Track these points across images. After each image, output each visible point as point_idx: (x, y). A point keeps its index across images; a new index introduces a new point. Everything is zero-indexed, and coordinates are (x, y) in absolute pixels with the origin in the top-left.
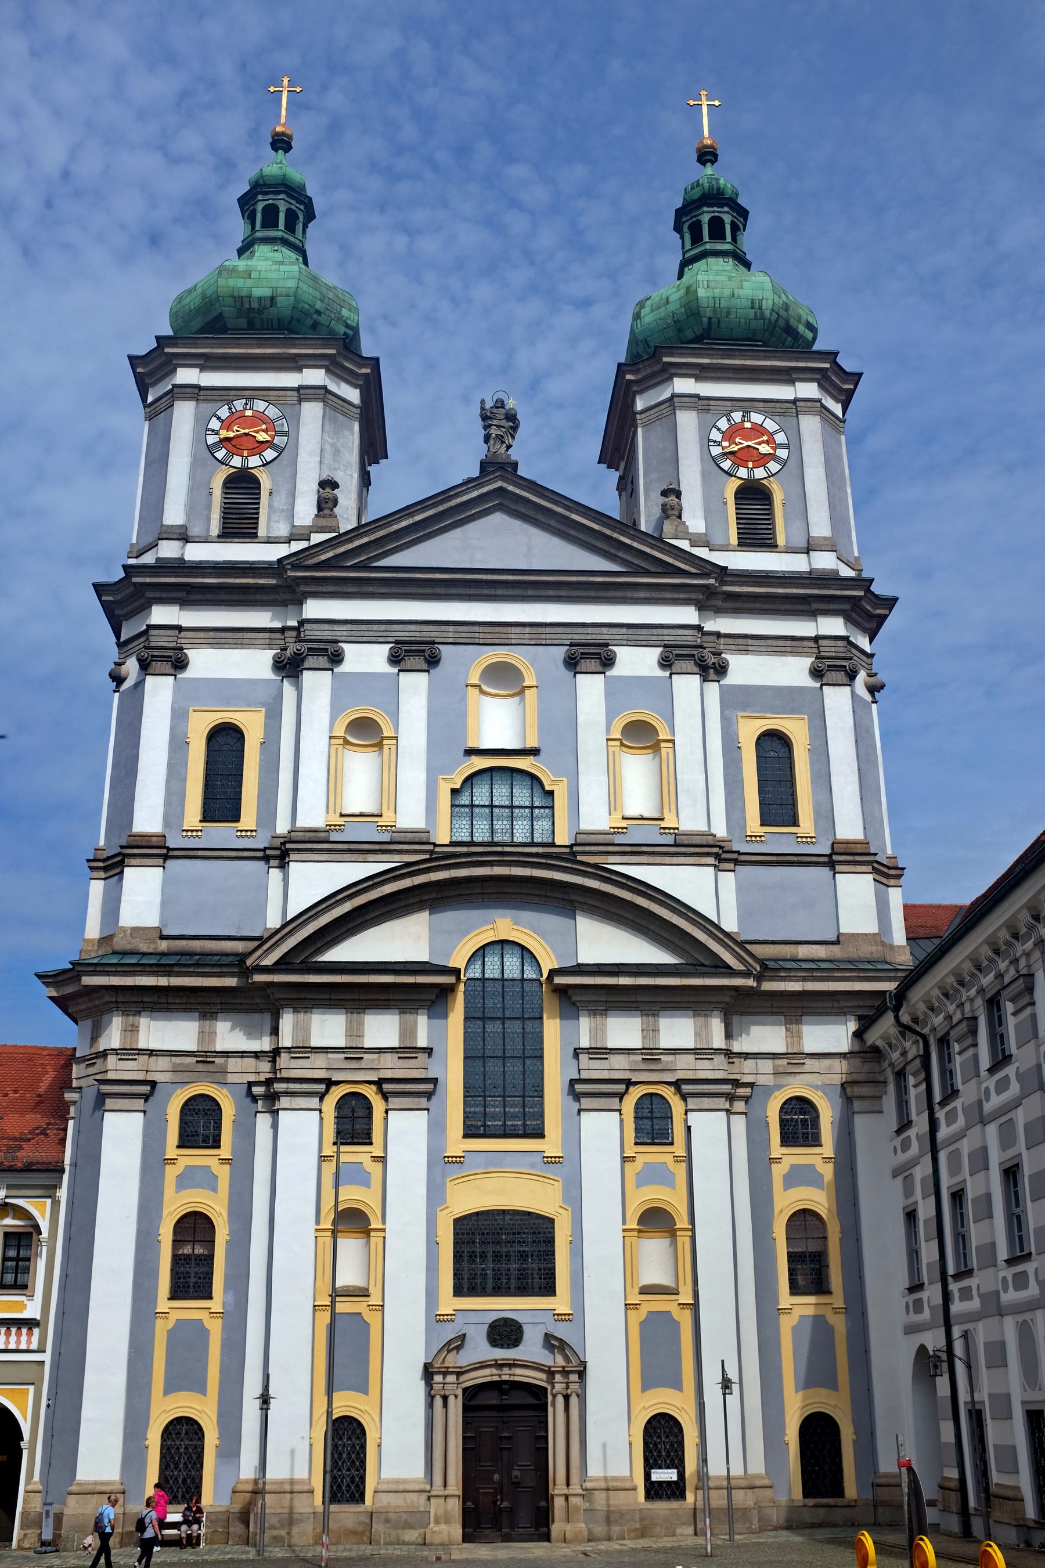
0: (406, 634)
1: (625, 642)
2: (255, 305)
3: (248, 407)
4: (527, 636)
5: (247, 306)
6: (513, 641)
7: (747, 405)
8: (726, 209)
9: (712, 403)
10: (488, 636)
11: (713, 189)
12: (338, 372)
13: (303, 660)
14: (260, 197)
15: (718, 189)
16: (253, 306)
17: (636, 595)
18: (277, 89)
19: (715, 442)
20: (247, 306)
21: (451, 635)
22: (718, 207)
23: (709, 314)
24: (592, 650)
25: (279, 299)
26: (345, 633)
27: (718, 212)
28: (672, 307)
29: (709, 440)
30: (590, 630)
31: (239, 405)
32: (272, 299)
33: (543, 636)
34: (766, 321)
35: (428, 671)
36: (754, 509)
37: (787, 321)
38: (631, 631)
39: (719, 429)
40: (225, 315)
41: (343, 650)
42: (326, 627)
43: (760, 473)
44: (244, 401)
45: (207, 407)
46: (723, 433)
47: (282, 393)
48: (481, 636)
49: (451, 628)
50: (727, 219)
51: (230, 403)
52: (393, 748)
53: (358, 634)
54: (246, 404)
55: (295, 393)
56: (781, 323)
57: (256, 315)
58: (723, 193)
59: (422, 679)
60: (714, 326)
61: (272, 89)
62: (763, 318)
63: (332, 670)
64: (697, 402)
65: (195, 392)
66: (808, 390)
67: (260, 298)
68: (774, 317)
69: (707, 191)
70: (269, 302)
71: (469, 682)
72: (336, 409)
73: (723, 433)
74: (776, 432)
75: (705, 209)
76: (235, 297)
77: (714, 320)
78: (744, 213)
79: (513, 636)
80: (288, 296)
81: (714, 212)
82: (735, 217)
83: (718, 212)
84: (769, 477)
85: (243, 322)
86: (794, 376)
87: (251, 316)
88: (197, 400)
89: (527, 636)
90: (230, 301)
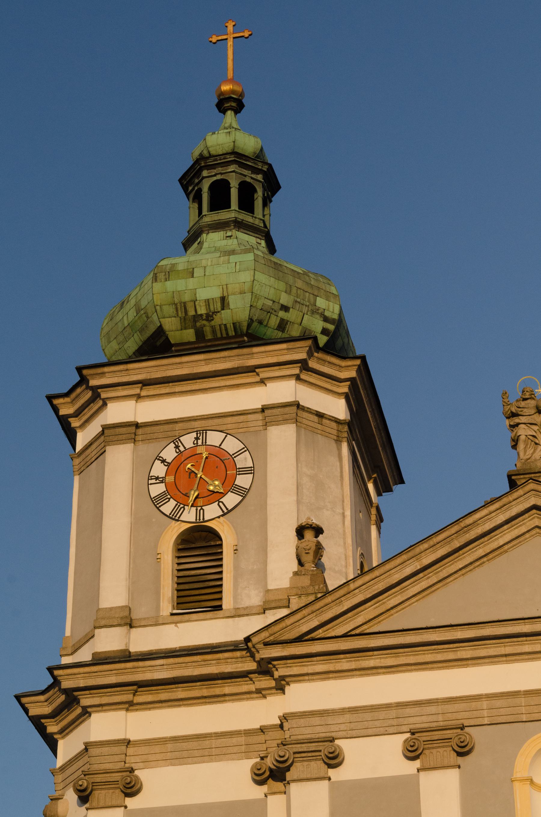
0: (424, 718)
2: (202, 310)
3: (200, 442)
5: (192, 313)
13: (288, 769)
16: (199, 312)
18: (220, 38)
20: (192, 313)
26: (343, 727)
40: (166, 327)
42: (316, 720)
47: (242, 418)
54: (197, 439)
55: (260, 416)
57: (205, 322)
61: (214, 39)
70: (219, 305)
76: (176, 305)
80: (242, 292)
85: (189, 335)
87: (198, 324)
88: (135, 441)
90: (169, 310)
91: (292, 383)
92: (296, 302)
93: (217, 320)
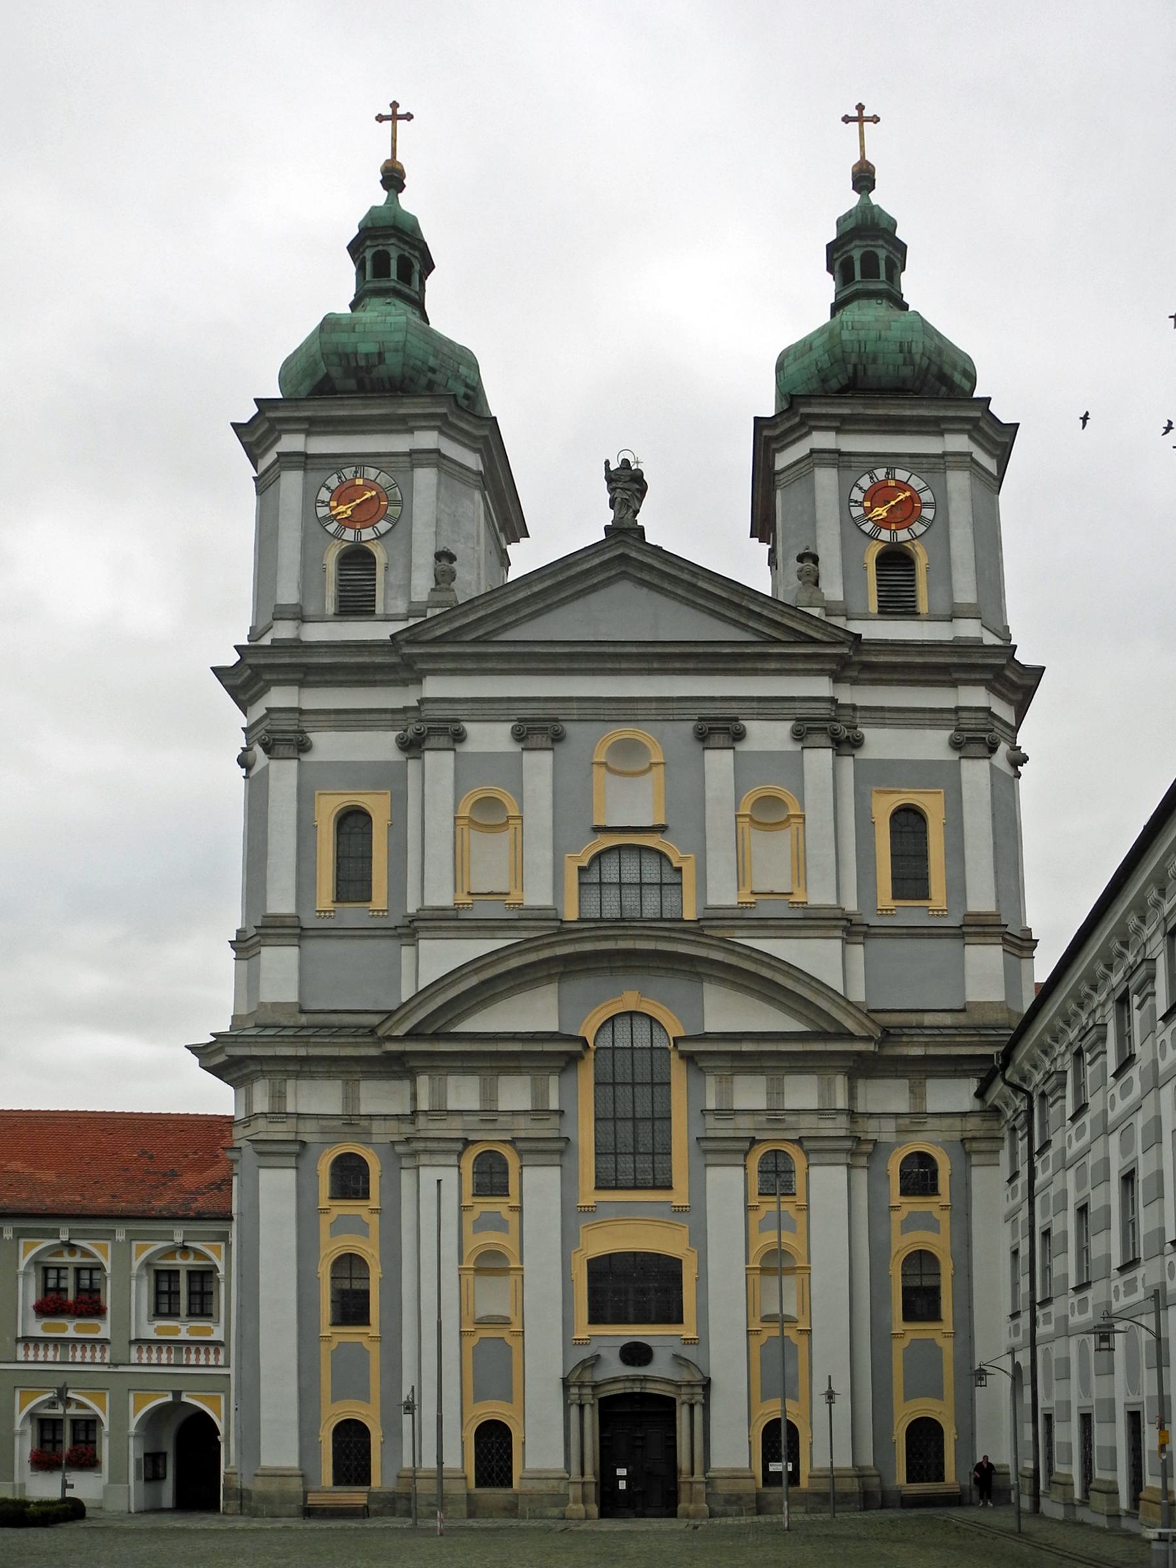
1: (755, 717)
2: (362, 363)
3: (358, 475)
4: (653, 712)
5: (354, 364)
6: (639, 717)
7: (892, 460)
8: (881, 242)
9: (852, 459)
10: (614, 712)
11: (866, 219)
12: (452, 433)
13: (424, 740)
14: (368, 243)
15: (873, 218)
17: (766, 666)
19: (856, 502)
20: (354, 364)
21: (575, 711)
22: (873, 240)
23: (854, 359)
24: (720, 725)
25: (387, 355)
26: (466, 712)
27: (872, 246)
28: (815, 355)
29: (851, 501)
30: (718, 705)
31: (348, 473)
32: (380, 355)
33: (671, 712)
34: (917, 367)
35: (552, 749)
36: (896, 576)
37: (940, 369)
38: (762, 705)
39: (861, 488)
41: (464, 730)
42: (446, 706)
43: (903, 535)
44: (354, 468)
45: (316, 477)
46: (865, 492)
47: (393, 459)
48: (607, 712)
49: (575, 705)
50: (882, 254)
51: (338, 471)
52: (519, 827)
53: (480, 712)
54: (356, 472)
55: (407, 459)
56: (934, 369)
58: (878, 224)
59: (546, 758)
60: (860, 373)
62: (912, 364)
63: (454, 750)
64: (839, 459)
65: (303, 461)
66: (958, 443)
67: (367, 355)
68: (925, 362)
69: (860, 222)
70: (377, 359)
71: (596, 760)
72: (451, 475)
73: (865, 492)
74: (923, 490)
75: (857, 242)
77: (860, 367)
78: (902, 248)
79: (639, 712)
80: (396, 350)
81: (867, 246)
82: (890, 252)
83: (872, 246)
84: (913, 539)
85: (352, 383)
86: (943, 426)
88: (305, 470)
89: (653, 712)
91: (435, 434)
92: (442, 366)
93: (375, 374)
